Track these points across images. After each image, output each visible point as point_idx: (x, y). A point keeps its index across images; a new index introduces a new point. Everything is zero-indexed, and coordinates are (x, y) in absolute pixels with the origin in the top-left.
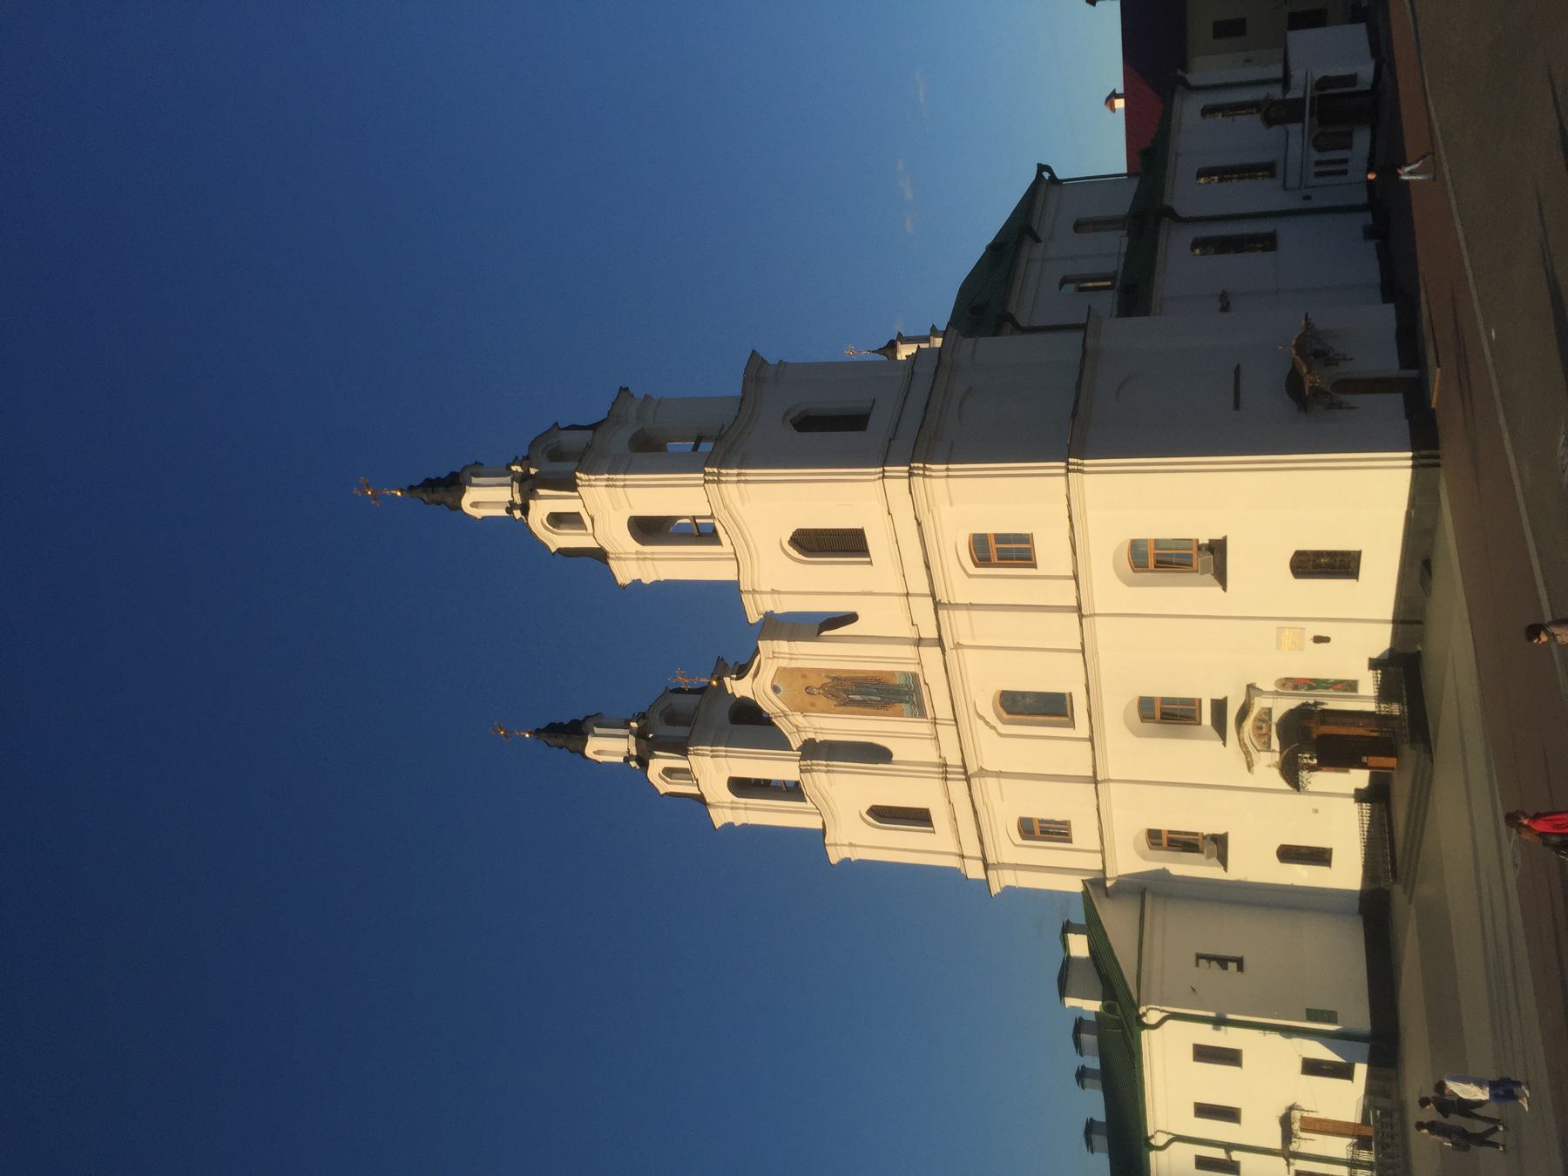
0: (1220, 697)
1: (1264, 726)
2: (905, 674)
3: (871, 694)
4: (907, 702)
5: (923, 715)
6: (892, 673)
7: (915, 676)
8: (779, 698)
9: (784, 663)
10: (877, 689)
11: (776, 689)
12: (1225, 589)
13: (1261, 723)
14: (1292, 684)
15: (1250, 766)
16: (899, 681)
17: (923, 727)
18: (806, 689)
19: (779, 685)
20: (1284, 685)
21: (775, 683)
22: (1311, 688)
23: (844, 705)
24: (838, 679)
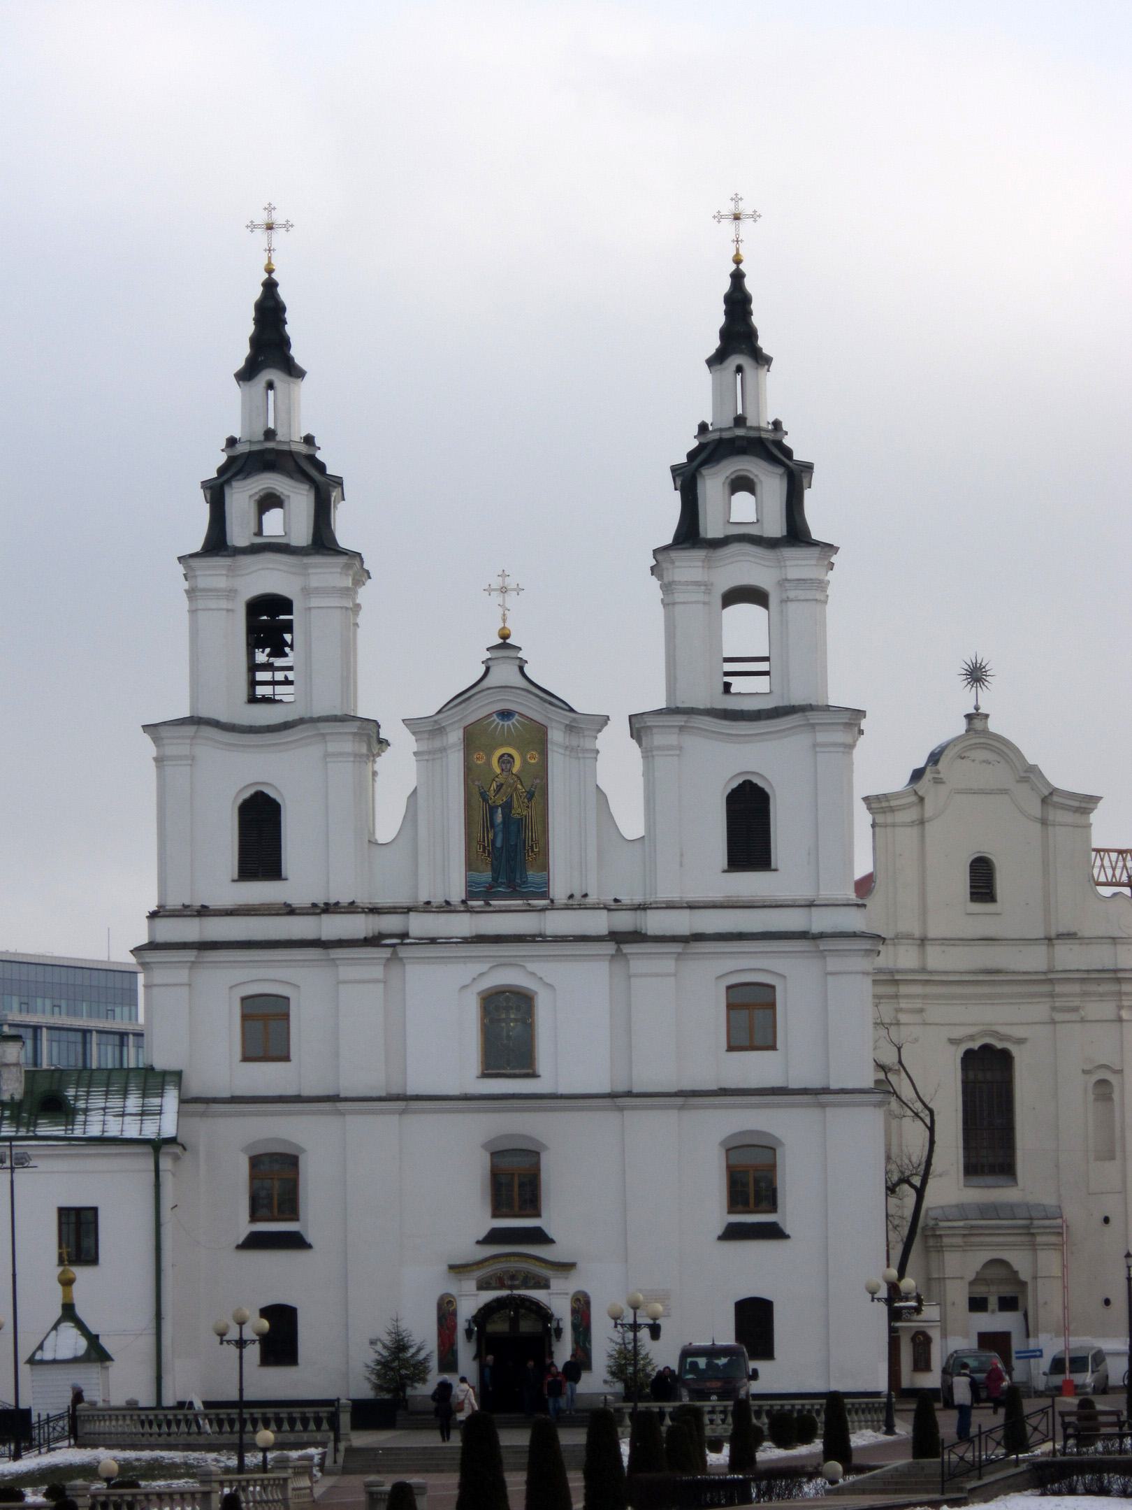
0: (551, 1233)
1: (517, 1283)
2: (547, 884)
3: (506, 839)
4: (495, 879)
5: (471, 895)
6: (545, 867)
7: (544, 895)
8: (490, 715)
9: (556, 736)
10: (516, 845)
11: (506, 714)
12: (720, 1238)
13: (521, 1278)
14: (582, 1308)
15: (457, 1269)
16: (532, 875)
17: (457, 892)
18: (510, 755)
19: (514, 720)
20: (578, 1300)
21: (517, 717)
22: (575, 1327)
23: (484, 796)
24: (530, 795)
